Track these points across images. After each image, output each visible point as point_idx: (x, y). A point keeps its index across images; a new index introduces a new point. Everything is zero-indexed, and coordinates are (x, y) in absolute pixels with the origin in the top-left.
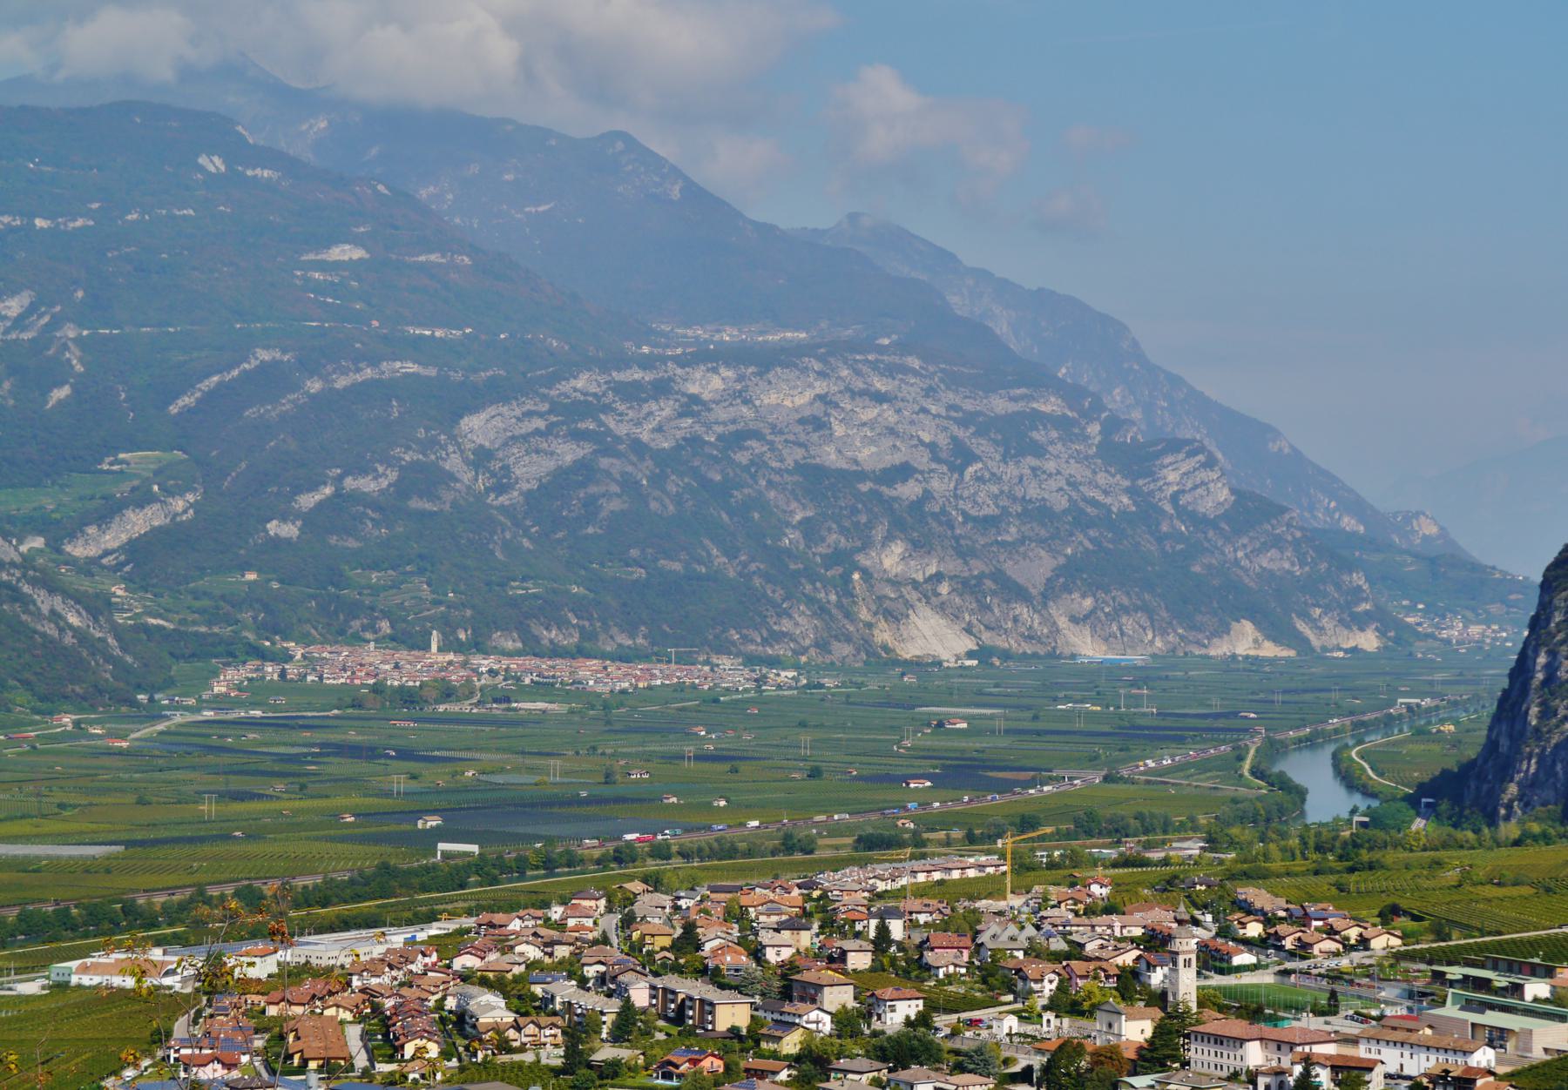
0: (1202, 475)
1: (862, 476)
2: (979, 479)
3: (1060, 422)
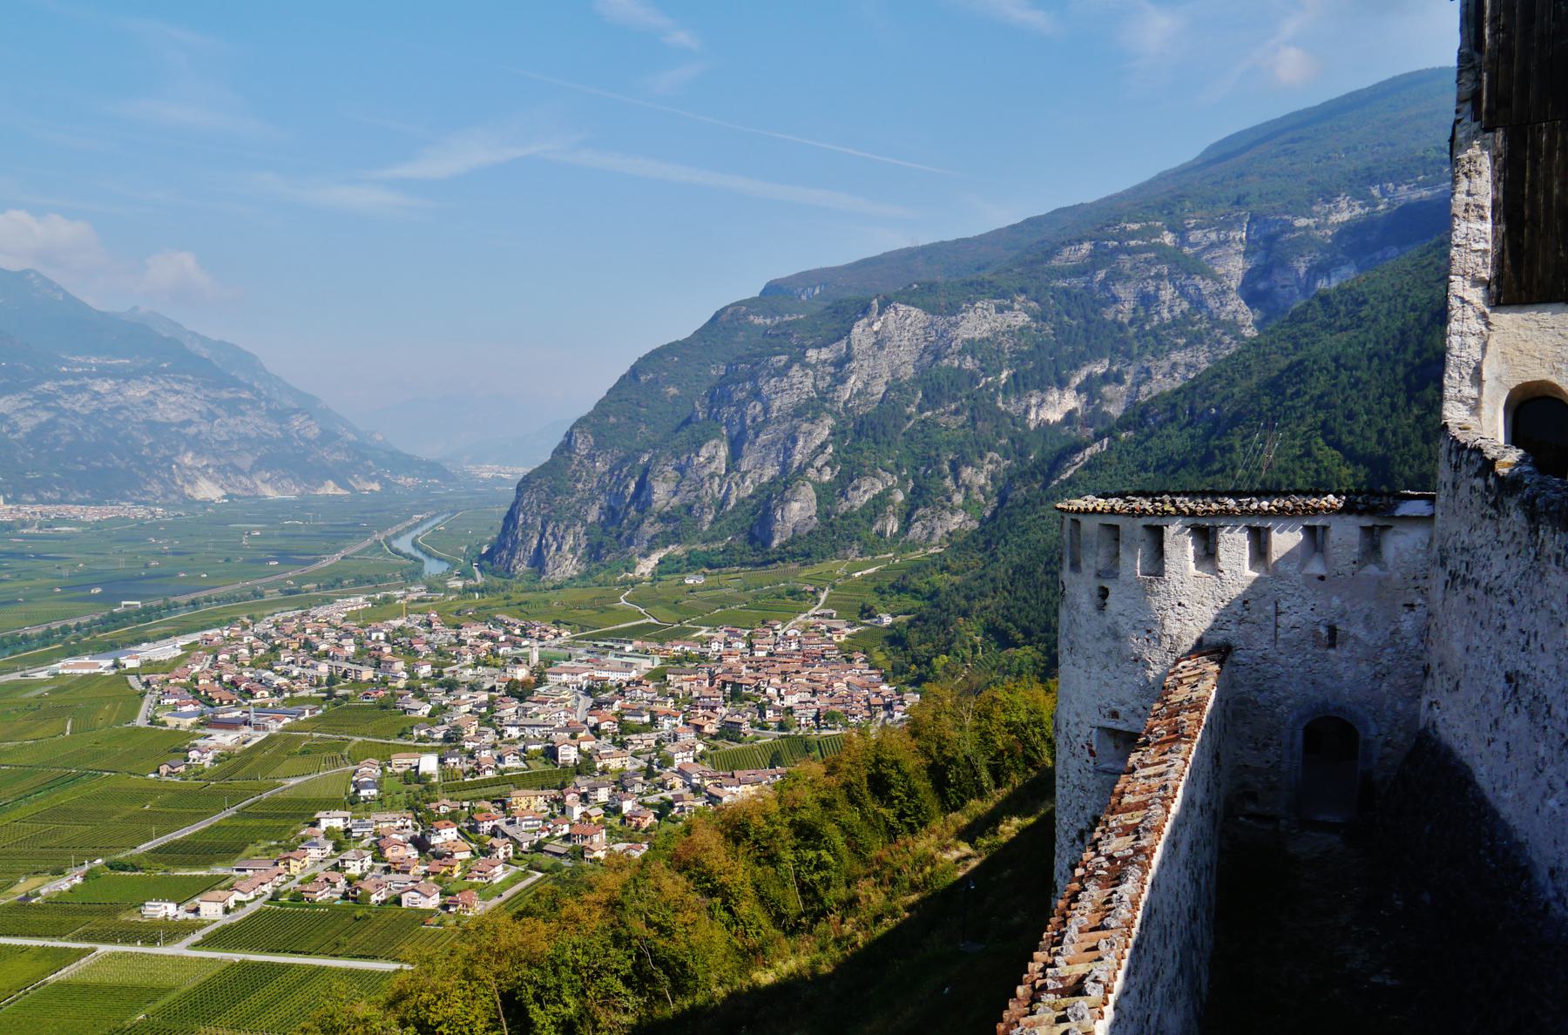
0: (307, 423)
1: (172, 424)
2: (220, 425)
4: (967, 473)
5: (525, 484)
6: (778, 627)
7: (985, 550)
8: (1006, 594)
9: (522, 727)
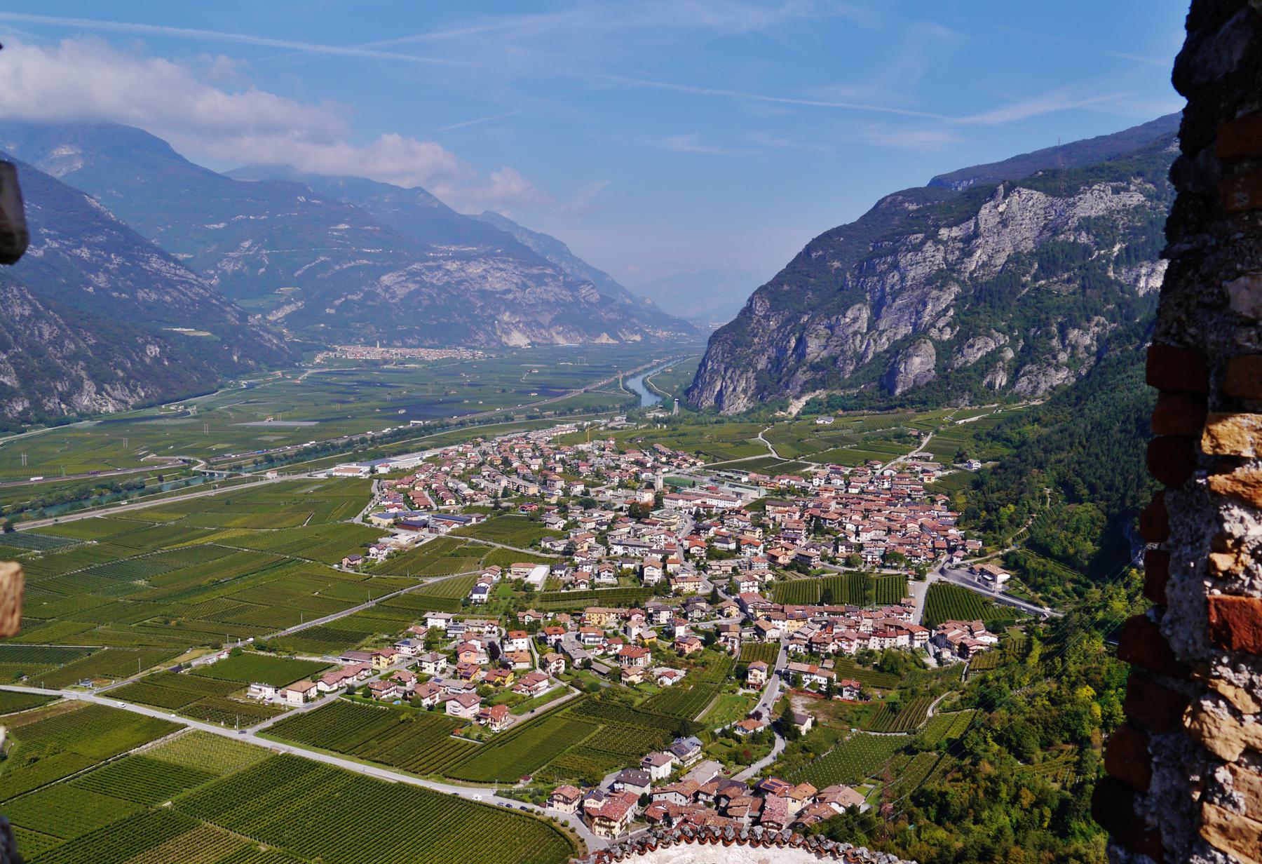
1: (497, 292)
3: (552, 276)
4: (1074, 334)
5: (716, 337)
6: (879, 466)
7: (1076, 405)
8: (1081, 449)
9: (626, 546)
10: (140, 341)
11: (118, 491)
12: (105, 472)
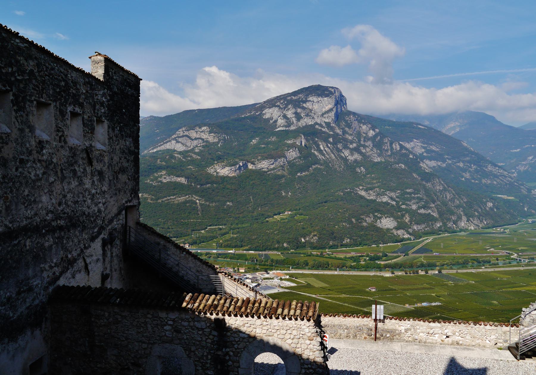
10: (484, 200)
11: (480, 262)
12: (473, 254)
